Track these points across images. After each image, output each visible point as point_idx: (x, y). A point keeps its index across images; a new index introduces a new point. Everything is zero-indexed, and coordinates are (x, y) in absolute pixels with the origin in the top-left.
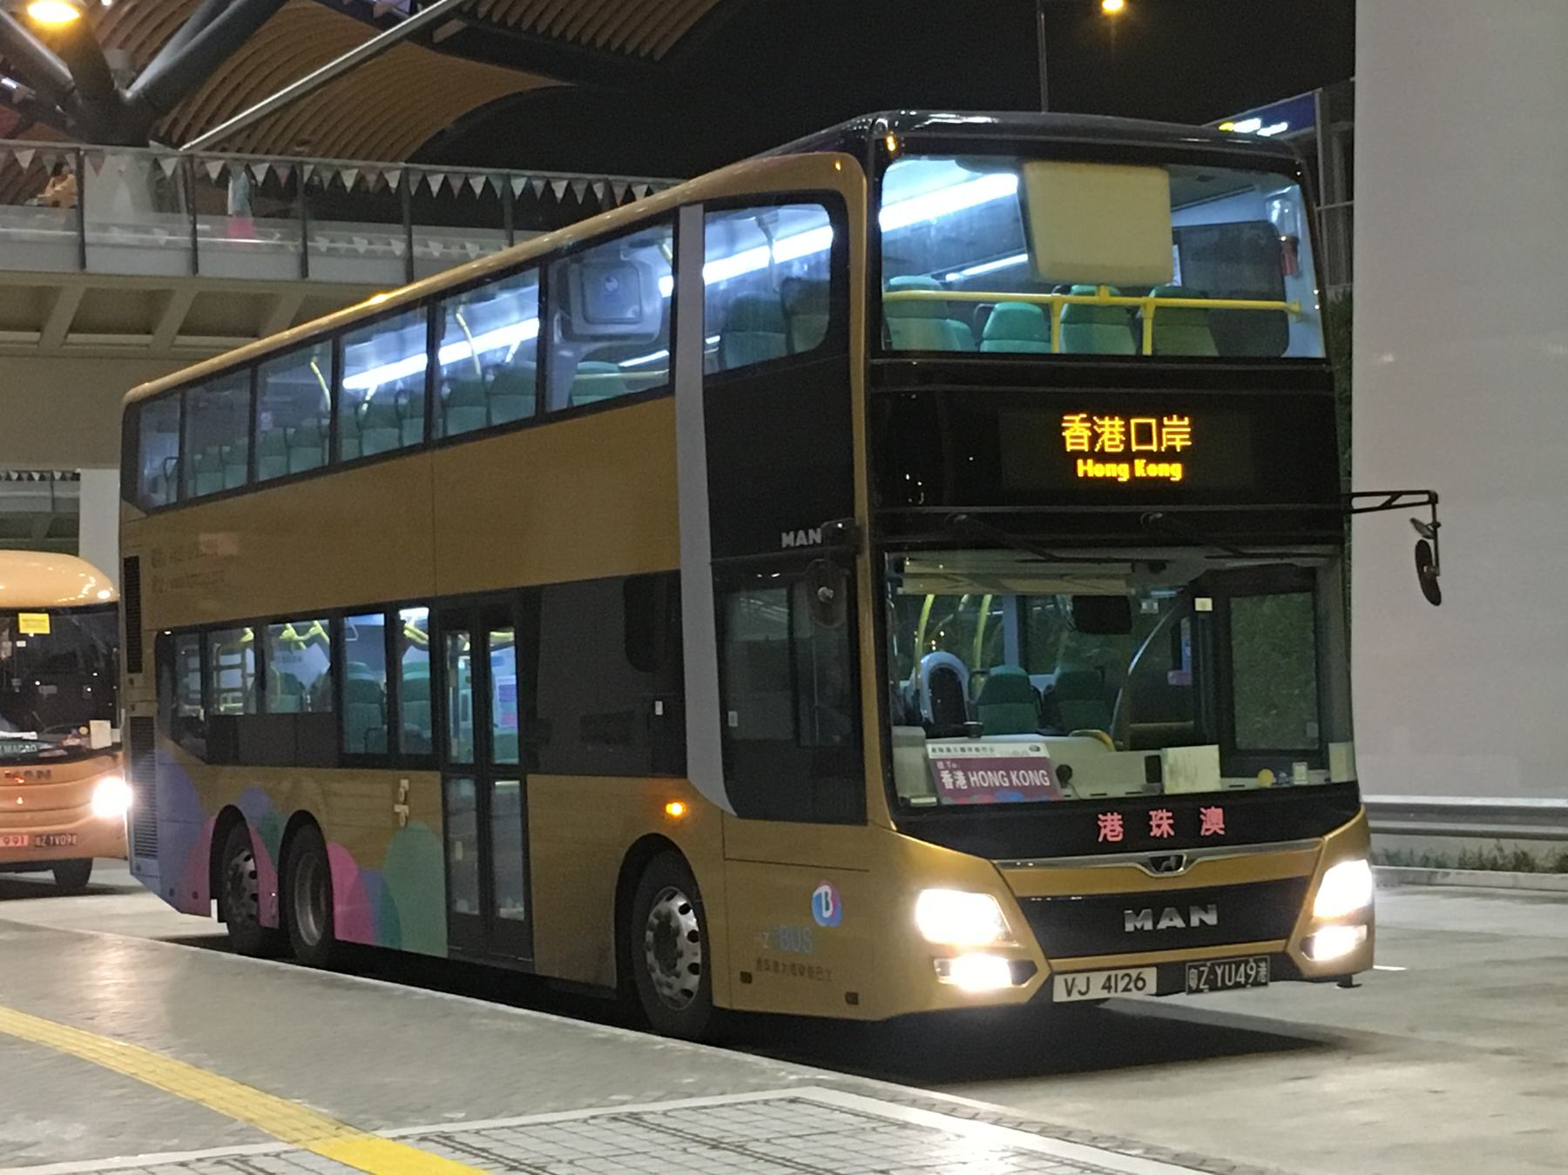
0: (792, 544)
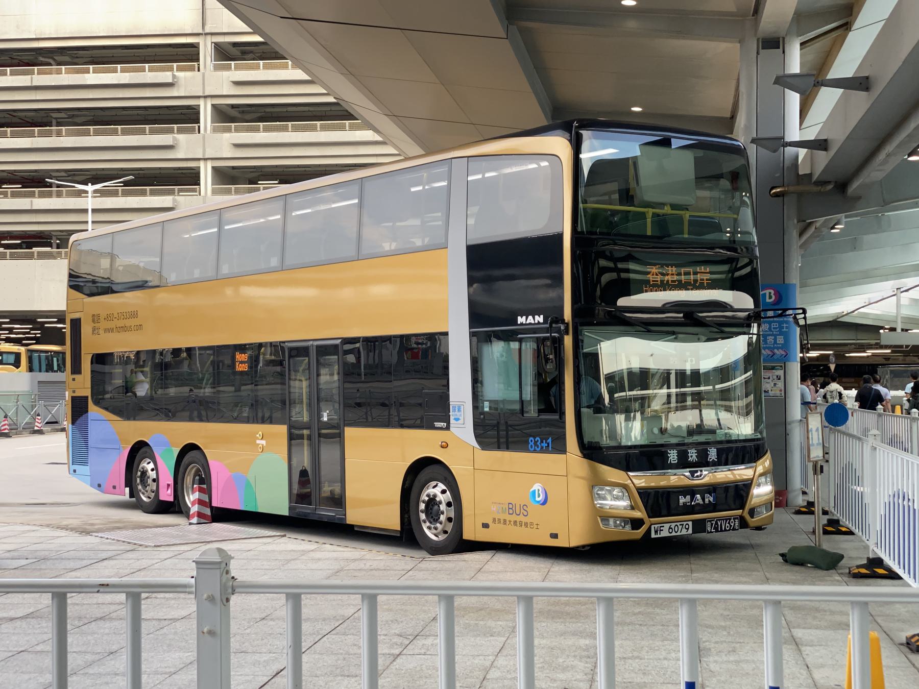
0: (524, 322)
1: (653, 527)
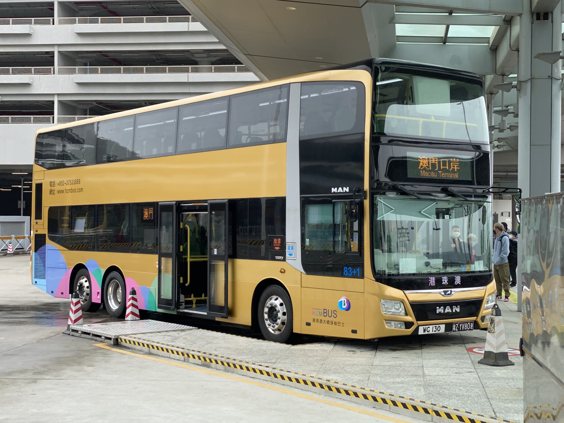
0: (336, 192)
1: (420, 327)
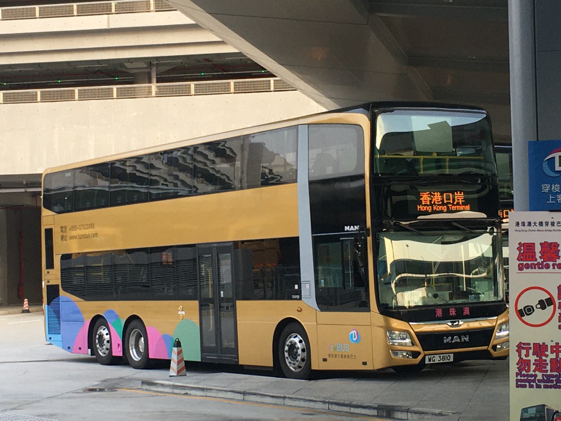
1: (427, 357)
